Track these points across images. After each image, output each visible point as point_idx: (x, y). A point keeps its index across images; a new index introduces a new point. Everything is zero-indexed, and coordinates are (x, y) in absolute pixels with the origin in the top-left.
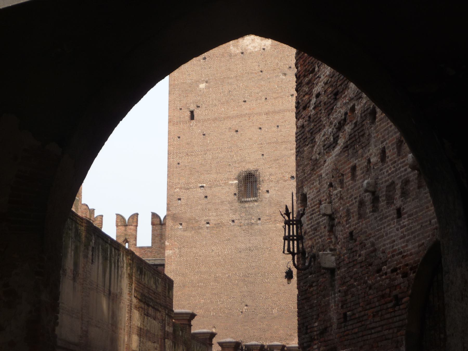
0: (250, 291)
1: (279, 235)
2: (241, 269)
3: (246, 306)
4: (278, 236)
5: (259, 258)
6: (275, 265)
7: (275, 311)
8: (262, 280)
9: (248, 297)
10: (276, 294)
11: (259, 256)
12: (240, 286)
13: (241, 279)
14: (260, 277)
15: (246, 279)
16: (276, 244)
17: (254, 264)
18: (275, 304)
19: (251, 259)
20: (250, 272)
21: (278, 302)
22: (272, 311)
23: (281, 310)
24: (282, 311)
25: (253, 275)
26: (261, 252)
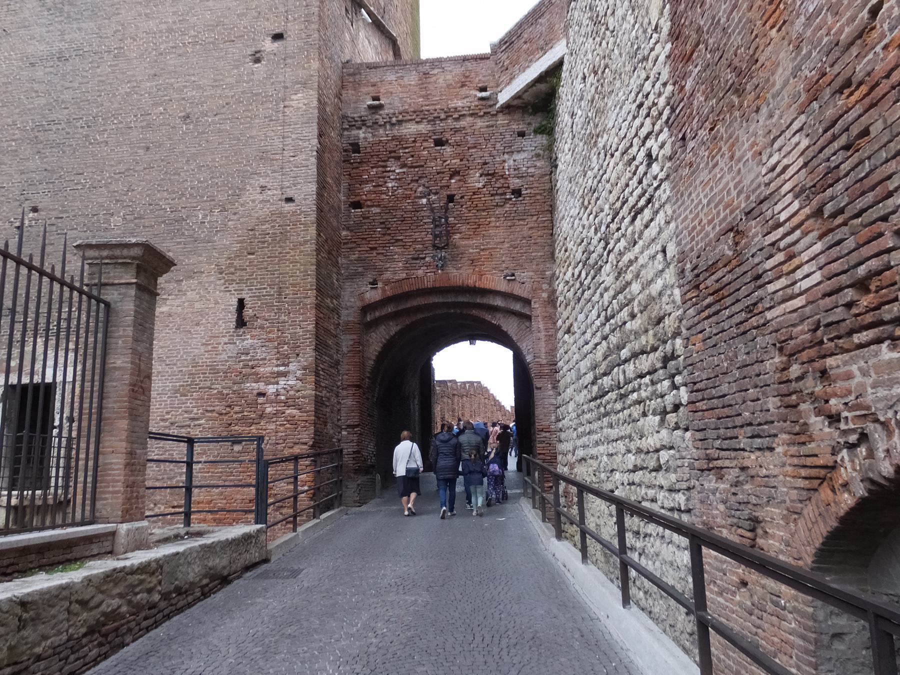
0: (49, 168)
1: (146, 15)
2: (29, 110)
3: (35, 210)
4: (144, 17)
5: (83, 77)
6: (128, 94)
7: (116, 220)
8: (87, 136)
9: (41, 186)
10: (123, 173)
11: (85, 74)
12: (21, 156)
13: (29, 139)
14: (80, 130)
15: (42, 136)
16: (135, 40)
17: (67, 96)
18: (117, 201)
19: (62, 82)
20: (53, 117)
21: (126, 195)
22: (107, 221)
23: (136, 218)
24: (136, 221)
25: (63, 125)
26: (91, 63)
